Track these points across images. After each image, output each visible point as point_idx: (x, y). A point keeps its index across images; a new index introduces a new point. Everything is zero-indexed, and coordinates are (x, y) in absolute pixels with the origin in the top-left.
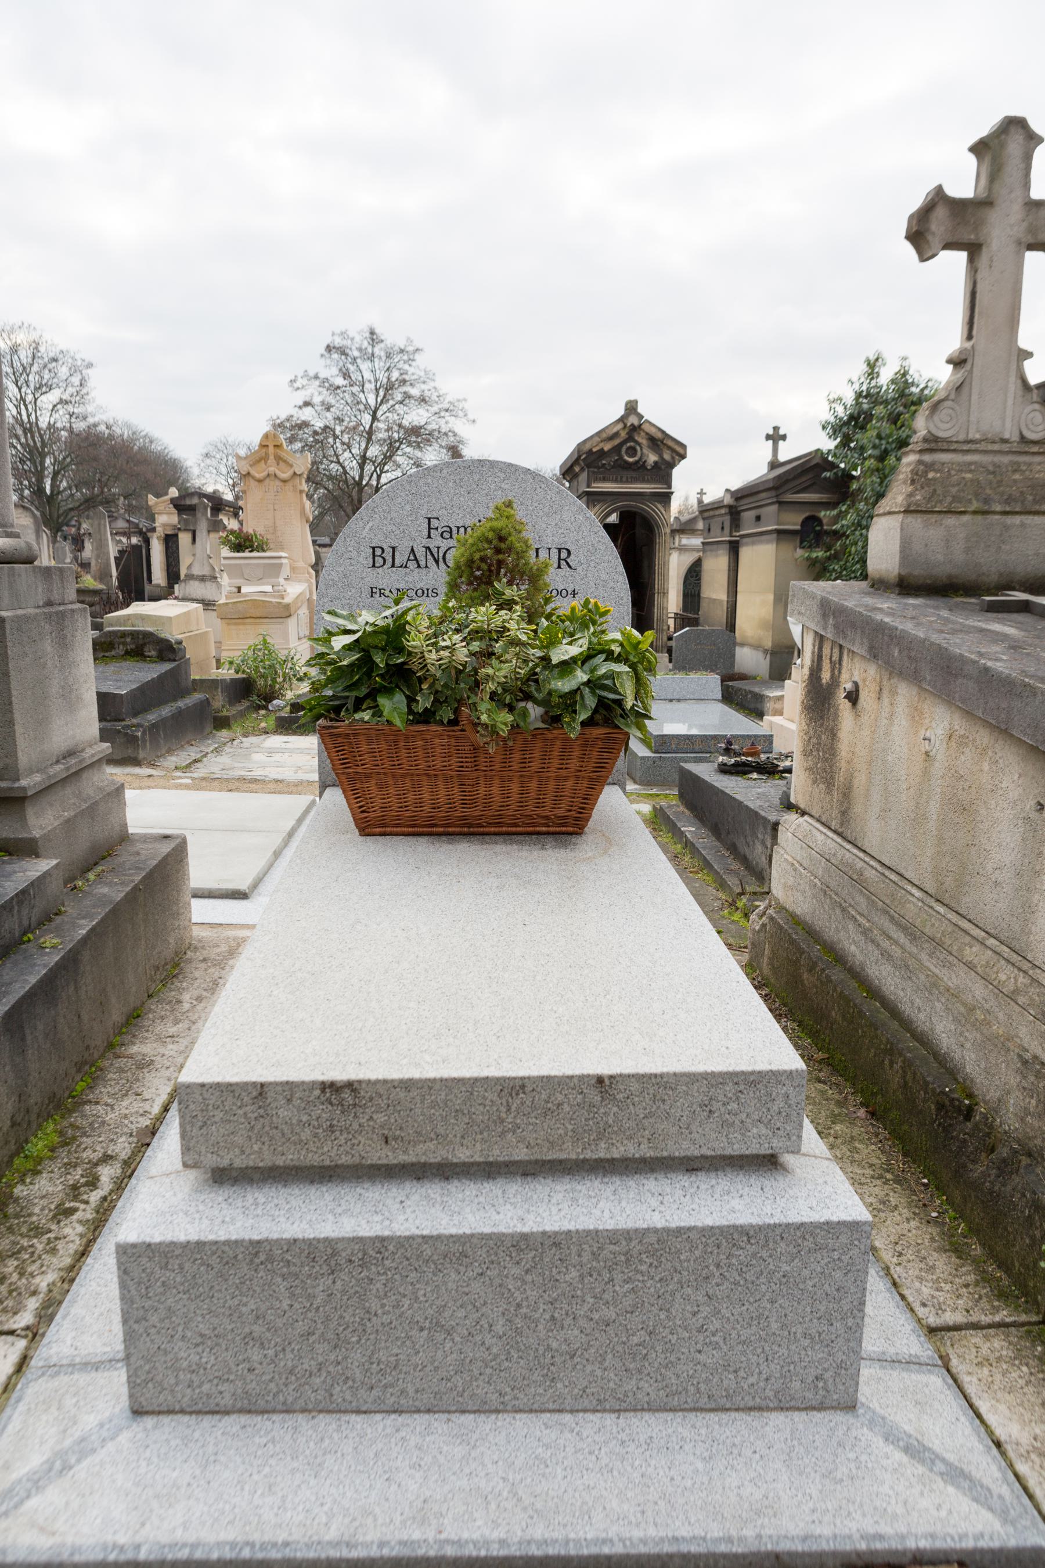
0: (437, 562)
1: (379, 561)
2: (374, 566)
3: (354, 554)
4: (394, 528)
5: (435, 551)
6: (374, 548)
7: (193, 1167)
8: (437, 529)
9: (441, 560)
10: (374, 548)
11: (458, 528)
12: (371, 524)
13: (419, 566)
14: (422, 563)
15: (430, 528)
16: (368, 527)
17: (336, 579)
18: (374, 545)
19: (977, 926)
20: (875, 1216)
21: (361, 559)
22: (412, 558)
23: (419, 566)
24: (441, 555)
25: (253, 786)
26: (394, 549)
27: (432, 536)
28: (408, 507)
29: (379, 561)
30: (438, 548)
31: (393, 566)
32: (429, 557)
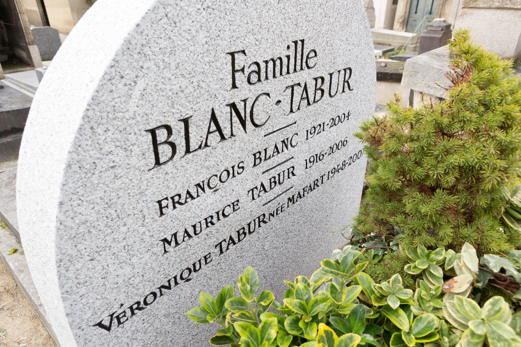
0: (243, 123)
1: (165, 151)
2: (158, 163)
3: (119, 156)
4: (184, 83)
5: (240, 107)
6: (153, 132)
7: (26, 296)
8: (243, 70)
9: (248, 118)
10: (153, 132)
11: (266, 62)
12: (141, 84)
13: (223, 138)
14: (226, 132)
15: (234, 71)
16: (136, 93)
17: (92, 217)
18: (153, 126)
19: (279, 165)
20: (303, 289)
21: (134, 161)
22: (213, 128)
23: (223, 138)
24: (248, 111)
25: (15, 278)
26: (186, 122)
27: (238, 83)
28: (202, 37)
29: (165, 151)
30: (245, 101)
31: (188, 151)
32: (235, 119)
